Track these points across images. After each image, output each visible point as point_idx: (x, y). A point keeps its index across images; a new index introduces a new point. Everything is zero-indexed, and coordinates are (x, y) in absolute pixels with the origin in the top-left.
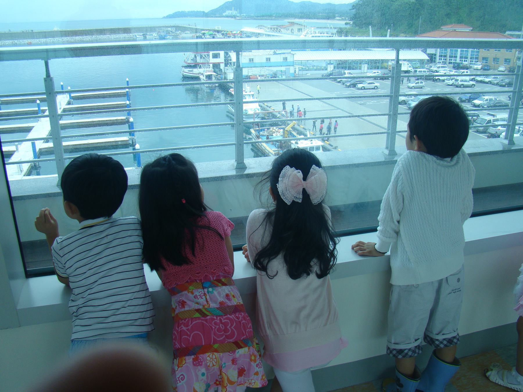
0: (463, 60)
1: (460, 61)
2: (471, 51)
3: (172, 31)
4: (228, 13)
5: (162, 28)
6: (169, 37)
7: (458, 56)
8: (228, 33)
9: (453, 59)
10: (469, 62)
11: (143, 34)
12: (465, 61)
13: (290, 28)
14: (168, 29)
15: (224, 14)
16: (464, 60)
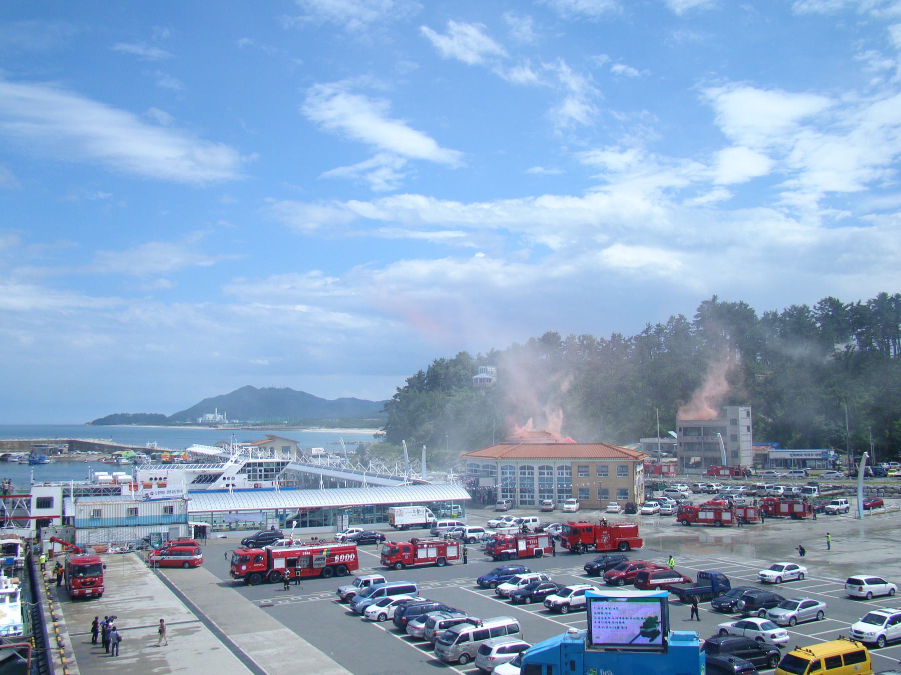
0: (546, 494)
1: (540, 498)
2: (558, 477)
3: (61, 451)
4: (210, 417)
5: (43, 444)
6: (48, 461)
7: (536, 489)
8: (163, 454)
9: (527, 494)
10: (557, 499)
11: (3, 454)
12: (548, 498)
13: (269, 446)
14: (52, 446)
15: (200, 420)
16: (547, 495)
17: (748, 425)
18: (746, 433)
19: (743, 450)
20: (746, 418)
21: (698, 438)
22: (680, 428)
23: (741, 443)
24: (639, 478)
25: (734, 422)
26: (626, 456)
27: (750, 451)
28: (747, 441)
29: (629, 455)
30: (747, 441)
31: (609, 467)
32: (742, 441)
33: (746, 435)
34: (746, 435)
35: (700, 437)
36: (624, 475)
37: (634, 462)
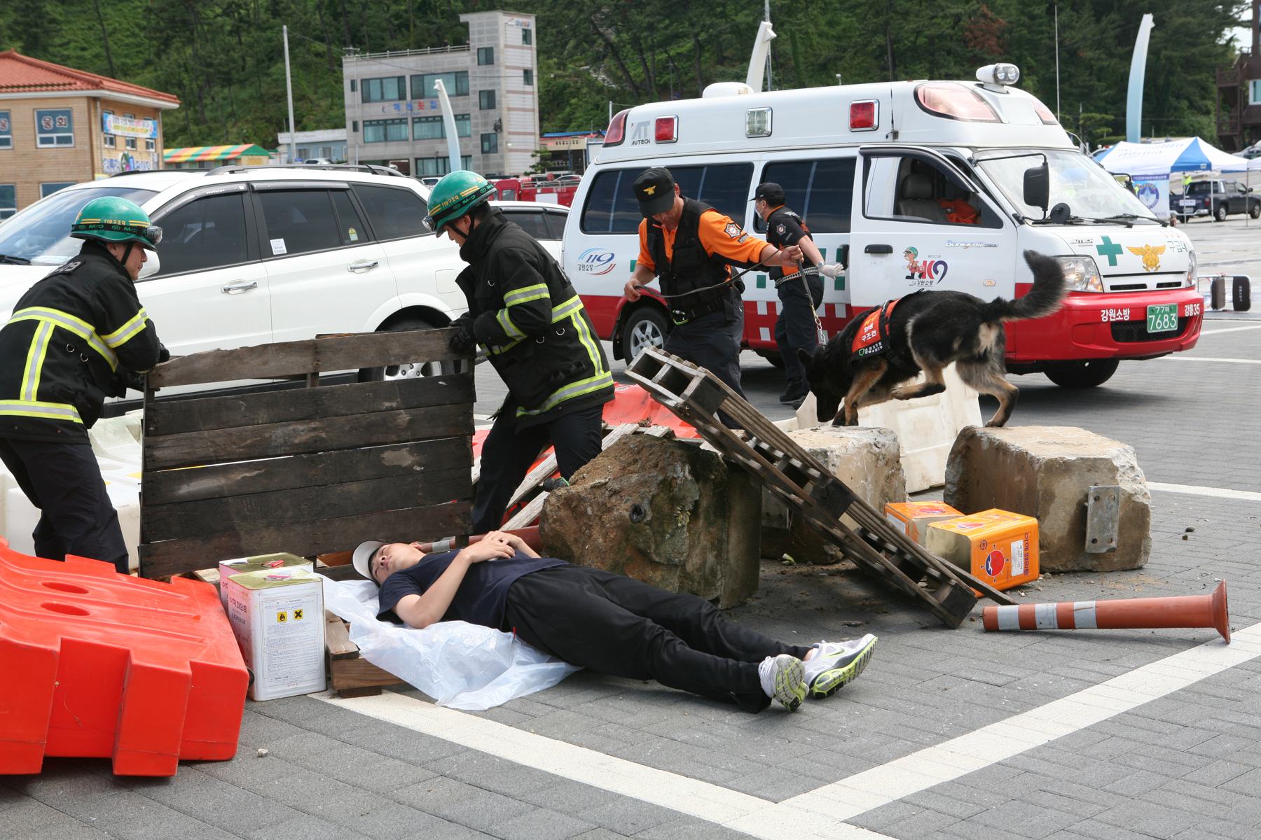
17: (528, 65)
18: (521, 89)
19: (510, 133)
20: (521, 48)
21: (397, 107)
22: (353, 83)
23: (505, 112)
24: (125, 156)
25: (487, 56)
26: (67, 80)
27: (533, 137)
28: (524, 110)
29: (77, 78)
30: (524, 110)
31: (14, 117)
32: (509, 109)
33: (524, 93)
34: (524, 93)
35: (403, 104)
36: (61, 140)
37: (94, 99)
